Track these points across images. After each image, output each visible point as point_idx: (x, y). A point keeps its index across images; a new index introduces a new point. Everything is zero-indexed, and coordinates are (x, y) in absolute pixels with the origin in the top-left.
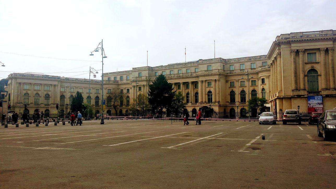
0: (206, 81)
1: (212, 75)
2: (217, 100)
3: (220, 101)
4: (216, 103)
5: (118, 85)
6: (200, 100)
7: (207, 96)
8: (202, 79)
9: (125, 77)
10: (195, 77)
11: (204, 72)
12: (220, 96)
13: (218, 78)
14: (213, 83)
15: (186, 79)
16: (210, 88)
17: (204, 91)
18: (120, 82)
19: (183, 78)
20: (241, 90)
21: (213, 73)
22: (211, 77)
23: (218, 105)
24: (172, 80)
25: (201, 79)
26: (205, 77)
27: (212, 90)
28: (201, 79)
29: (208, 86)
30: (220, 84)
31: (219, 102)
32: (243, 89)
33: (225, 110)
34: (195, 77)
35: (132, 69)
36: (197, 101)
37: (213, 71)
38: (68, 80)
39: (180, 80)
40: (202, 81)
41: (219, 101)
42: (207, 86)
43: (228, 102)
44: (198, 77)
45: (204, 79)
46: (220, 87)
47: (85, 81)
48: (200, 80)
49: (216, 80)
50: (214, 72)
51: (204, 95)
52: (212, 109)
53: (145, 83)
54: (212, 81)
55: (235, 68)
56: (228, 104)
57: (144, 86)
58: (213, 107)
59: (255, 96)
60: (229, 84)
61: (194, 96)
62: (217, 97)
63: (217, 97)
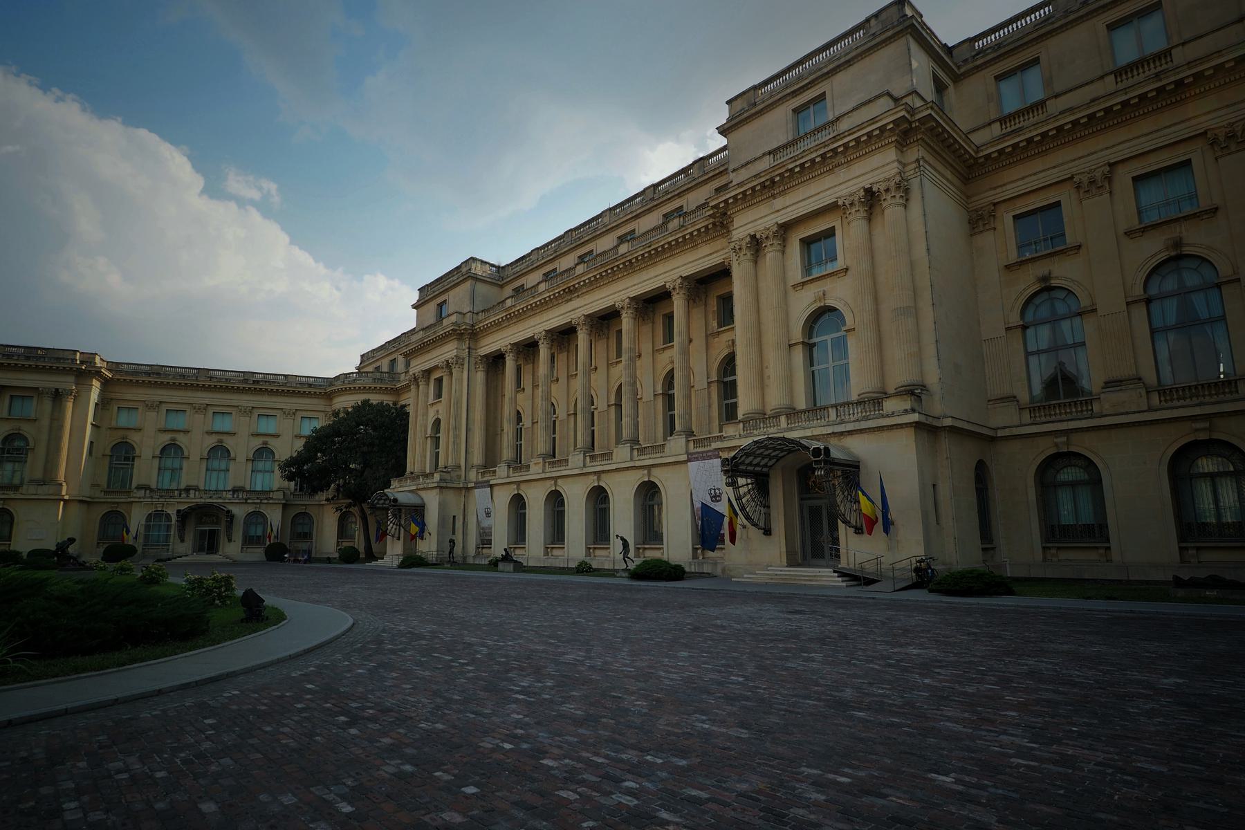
0: (785, 228)
1: (829, 160)
2: (899, 376)
3: (932, 377)
4: (890, 405)
6: (745, 403)
7: (799, 355)
12: (928, 338)
13: (893, 169)
14: (849, 238)
16: (827, 285)
17: (769, 317)
19: (631, 266)
20: (1154, 262)
22: (828, 181)
23: (915, 417)
26: (779, 203)
27: (840, 293)
29: (807, 269)
30: (918, 228)
31: (915, 392)
32: (1178, 244)
33: (981, 474)
36: (730, 413)
37: (844, 126)
38: (158, 374)
40: (756, 244)
41: (923, 387)
42: (796, 274)
43: (1013, 398)
44: (720, 223)
46: (920, 250)
47: (246, 381)
49: (871, 198)
51: (773, 359)
52: (851, 471)
54: (837, 224)
55: (1047, 83)
56: (1004, 419)
57: (448, 365)
58: (858, 447)
60: (1002, 241)
62: (897, 353)
63: (897, 353)
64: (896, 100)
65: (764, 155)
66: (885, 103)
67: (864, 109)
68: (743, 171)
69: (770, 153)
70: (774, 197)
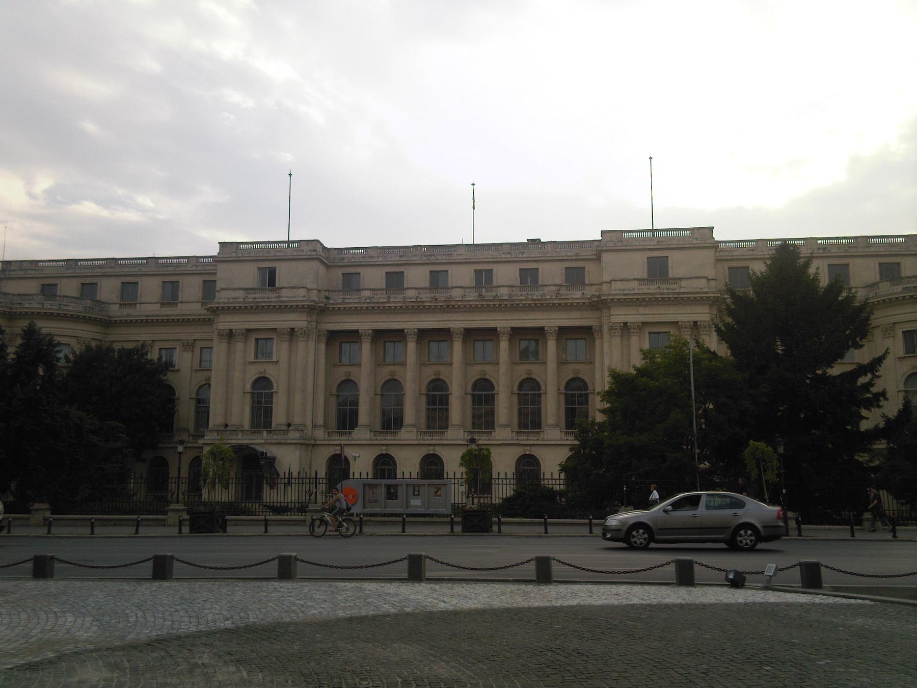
5: (108, 323)
8: (622, 319)
9: (150, 289)
10: (579, 307)
11: (635, 284)
15: (532, 315)
18: (115, 311)
21: (682, 290)
24: (454, 316)
25: (619, 315)
26: (641, 310)
28: (619, 315)
34: (579, 307)
35: (215, 251)
37: (683, 283)
39: (500, 316)
45: (633, 316)
48: (615, 319)
50: (687, 286)
53: (298, 321)
59: (487, 403)
61: (469, 398)
64: (708, 280)
65: (634, 279)
66: (705, 281)
67: (695, 281)
68: (619, 283)
69: (637, 280)
70: (640, 306)
